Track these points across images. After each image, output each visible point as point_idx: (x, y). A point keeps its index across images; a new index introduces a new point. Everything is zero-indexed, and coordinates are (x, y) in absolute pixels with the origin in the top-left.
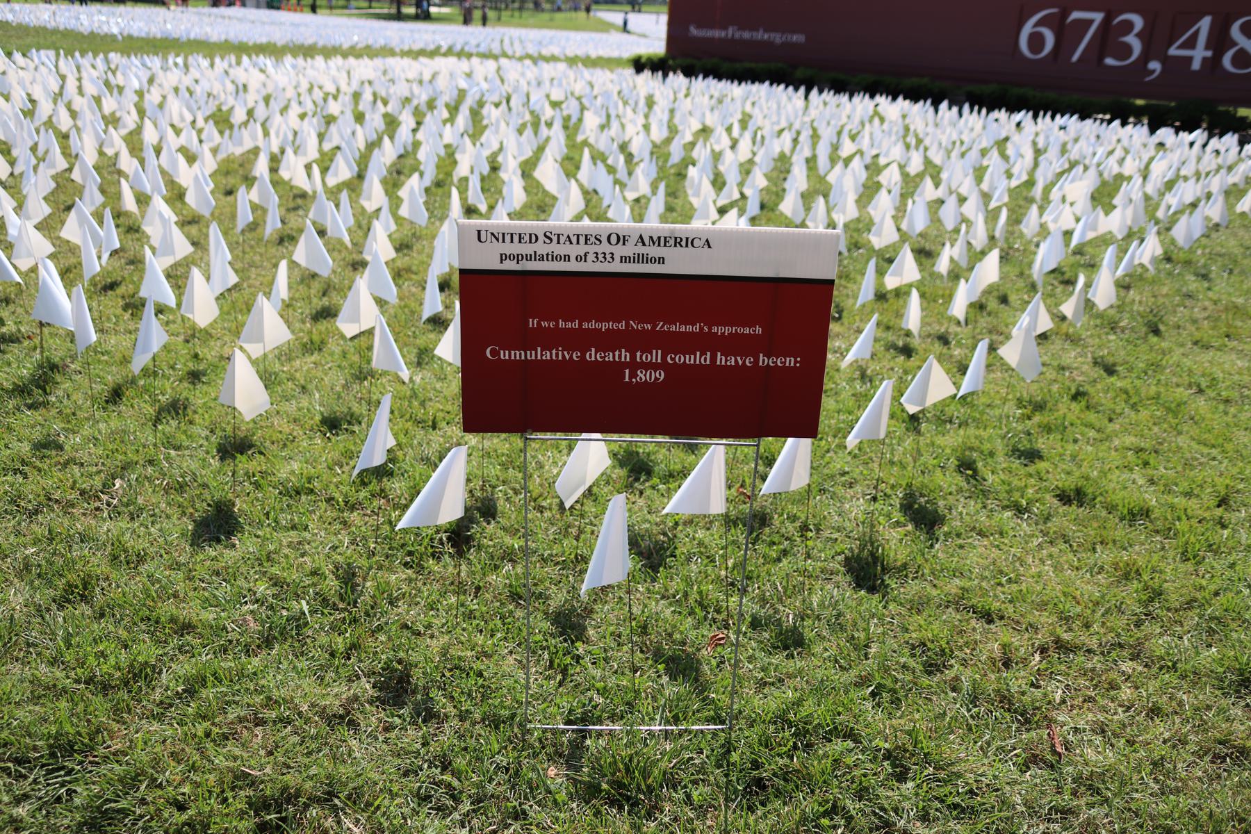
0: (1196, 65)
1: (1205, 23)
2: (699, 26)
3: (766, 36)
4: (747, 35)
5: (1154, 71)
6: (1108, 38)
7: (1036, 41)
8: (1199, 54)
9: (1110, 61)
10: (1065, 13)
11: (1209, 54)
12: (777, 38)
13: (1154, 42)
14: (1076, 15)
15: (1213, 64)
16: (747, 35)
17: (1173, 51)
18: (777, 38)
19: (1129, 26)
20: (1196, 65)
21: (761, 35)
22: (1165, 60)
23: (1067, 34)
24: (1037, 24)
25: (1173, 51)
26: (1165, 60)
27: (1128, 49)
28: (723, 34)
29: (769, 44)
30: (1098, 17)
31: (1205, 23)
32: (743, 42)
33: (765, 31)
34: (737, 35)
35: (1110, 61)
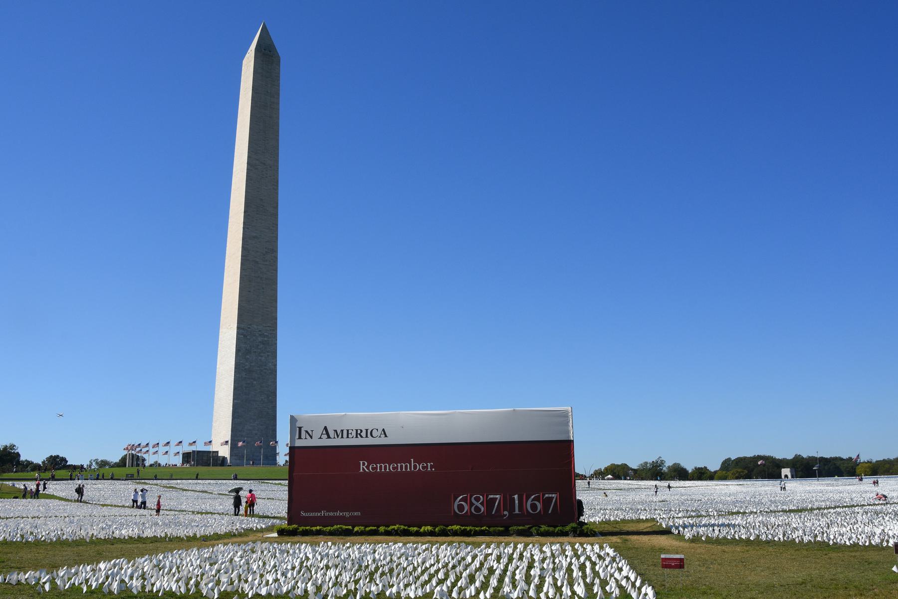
4: (331, 514)
16: (331, 514)
34: (327, 514)
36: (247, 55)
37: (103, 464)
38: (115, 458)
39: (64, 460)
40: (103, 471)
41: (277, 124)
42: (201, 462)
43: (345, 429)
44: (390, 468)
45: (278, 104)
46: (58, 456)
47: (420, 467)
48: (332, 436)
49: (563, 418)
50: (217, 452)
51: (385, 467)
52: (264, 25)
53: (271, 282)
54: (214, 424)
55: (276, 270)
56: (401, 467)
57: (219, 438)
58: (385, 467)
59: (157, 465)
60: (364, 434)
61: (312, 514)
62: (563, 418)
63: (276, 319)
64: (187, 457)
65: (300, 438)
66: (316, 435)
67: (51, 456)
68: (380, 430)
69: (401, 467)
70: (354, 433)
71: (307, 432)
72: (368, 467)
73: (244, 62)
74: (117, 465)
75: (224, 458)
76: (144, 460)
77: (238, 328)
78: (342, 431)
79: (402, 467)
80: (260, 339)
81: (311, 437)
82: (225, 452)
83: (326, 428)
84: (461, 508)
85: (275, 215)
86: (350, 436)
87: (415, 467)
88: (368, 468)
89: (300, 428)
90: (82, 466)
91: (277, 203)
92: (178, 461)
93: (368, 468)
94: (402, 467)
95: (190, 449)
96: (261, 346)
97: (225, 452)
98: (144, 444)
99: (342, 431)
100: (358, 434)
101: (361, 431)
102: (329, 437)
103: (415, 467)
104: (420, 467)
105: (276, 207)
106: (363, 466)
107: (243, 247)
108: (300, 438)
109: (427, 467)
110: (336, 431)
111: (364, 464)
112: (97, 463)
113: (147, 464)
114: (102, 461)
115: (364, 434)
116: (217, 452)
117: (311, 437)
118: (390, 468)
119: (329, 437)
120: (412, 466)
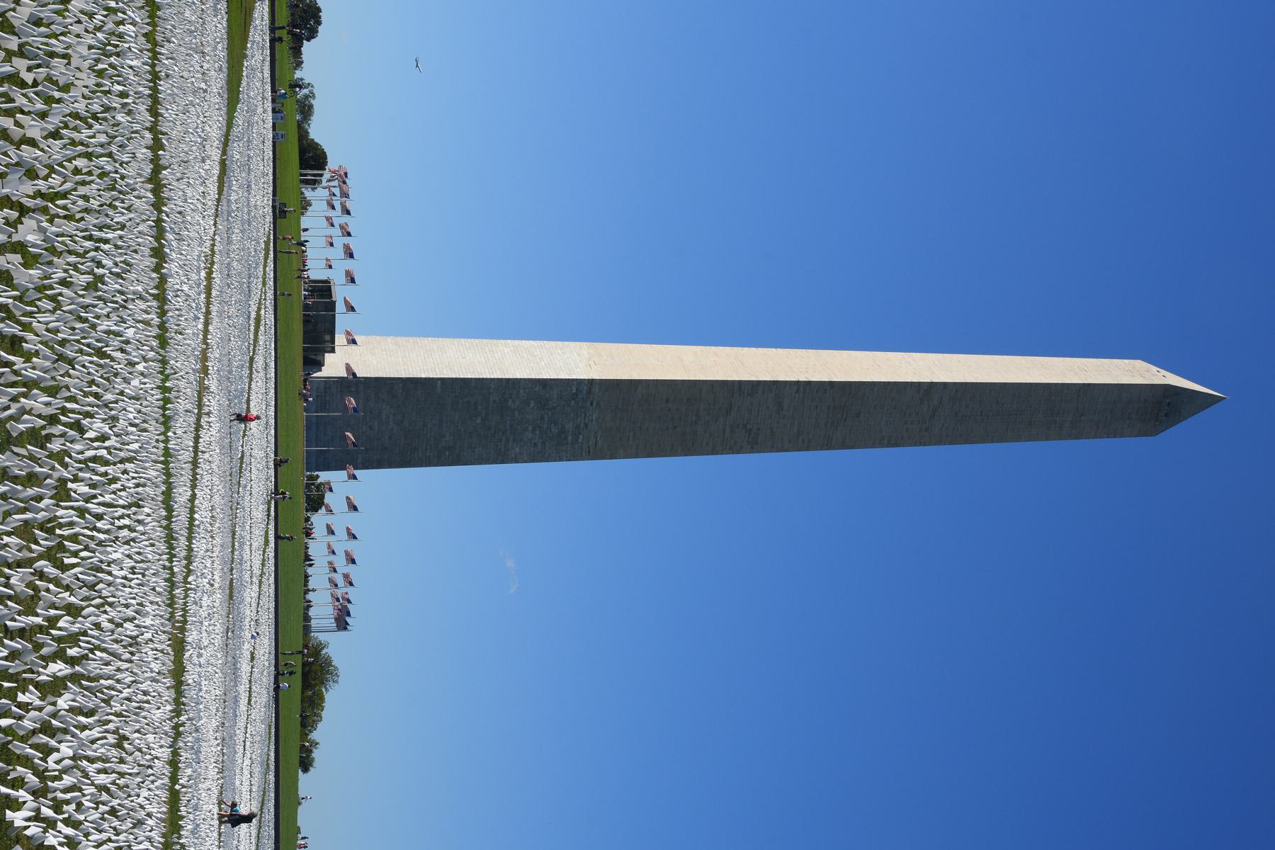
36: (1154, 369)
37: (306, 110)
38: (318, 131)
39: (312, 34)
40: (292, 104)
41: (1017, 438)
42: (311, 319)
45: (1060, 437)
46: (319, 23)
50: (333, 351)
52: (1215, 400)
53: (687, 444)
54: (389, 339)
55: (714, 452)
57: (366, 352)
59: (305, 205)
63: (611, 458)
64: (323, 290)
67: (319, 10)
73: (1139, 363)
74: (303, 135)
75: (319, 365)
76: (314, 183)
77: (591, 382)
80: (570, 426)
82: (333, 366)
85: (828, 445)
90: (299, 64)
91: (852, 447)
92: (316, 272)
95: (340, 293)
96: (555, 430)
97: (333, 366)
98: (349, 205)
105: (844, 446)
107: (759, 382)
112: (307, 97)
113: (308, 193)
114: (311, 107)
116: (333, 351)
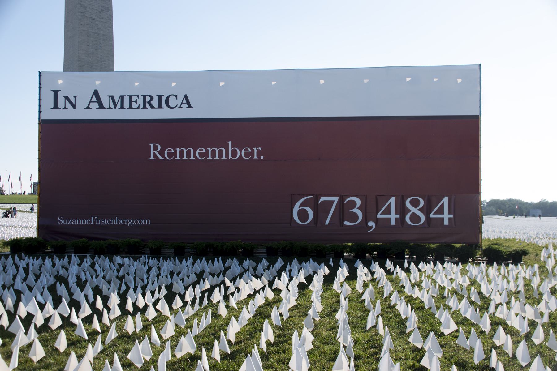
0: (393, 223)
1: (392, 200)
2: (65, 218)
3: (121, 222)
4: (105, 222)
5: (372, 227)
6: (343, 210)
7: (303, 215)
8: (393, 217)
9: (346, 223)
10: (317, 198)
11: (398, 216)
12: (130, 222)
13: (370, 210)
14: (323, 199)
15: (401, 221)
16: (105, 222)
17: (379, 216)
18: (130, 222)
19: (353, 204)
20: (393, 223)
21: (116, 221)
22: (377, 221)
23: (320, 210)
24: (302, 205)
25: (379, 216)
26: (377, 221)
27: (356, 216)
28: (86, 222)
29: (125, 226)
30: (336, 199)
31: (392, 200)
32: (102, 226)
33: (120, 218)
34: (98, 222)
35: (346, 223)
43: (126, 93)
44: (196, 154)
47: (241, 153)
48: (106, 101)
49: (472, 75)
51: (189, 153)
56: (213, 152)
58: (189, 153)
60: (155, 103)
61: (75, 222)
62: (472, 75)
65: (56, 106)
66: (82, 103)
68: (181, 97)
69: (213, 152)
70: (140, 101)
71: (66, 98)
72: (162, 153)
78: (122, 97)
79: (214, 153)
81: (74, 106)
83: (96, 93)
84: (303, 215)
86: (134, 105)
87: (234, 153)
88: (163, 156)
89: (56, 93)
93: (163, 156)
94: (214, 153)
99: (122, 97)
100: (147, 102)
101: (152, 98)
102: (101, 106)
103: (234, 153)
104: (241, 153)
106: (154, 152)
108: (56, 106)
109: (252, 153)
110: (112, 97)
111: (155, 148)
115: (155, 103)
117: (74, 106)
118: (196, 154)
119: (101, 106)
120: (230, 152)
